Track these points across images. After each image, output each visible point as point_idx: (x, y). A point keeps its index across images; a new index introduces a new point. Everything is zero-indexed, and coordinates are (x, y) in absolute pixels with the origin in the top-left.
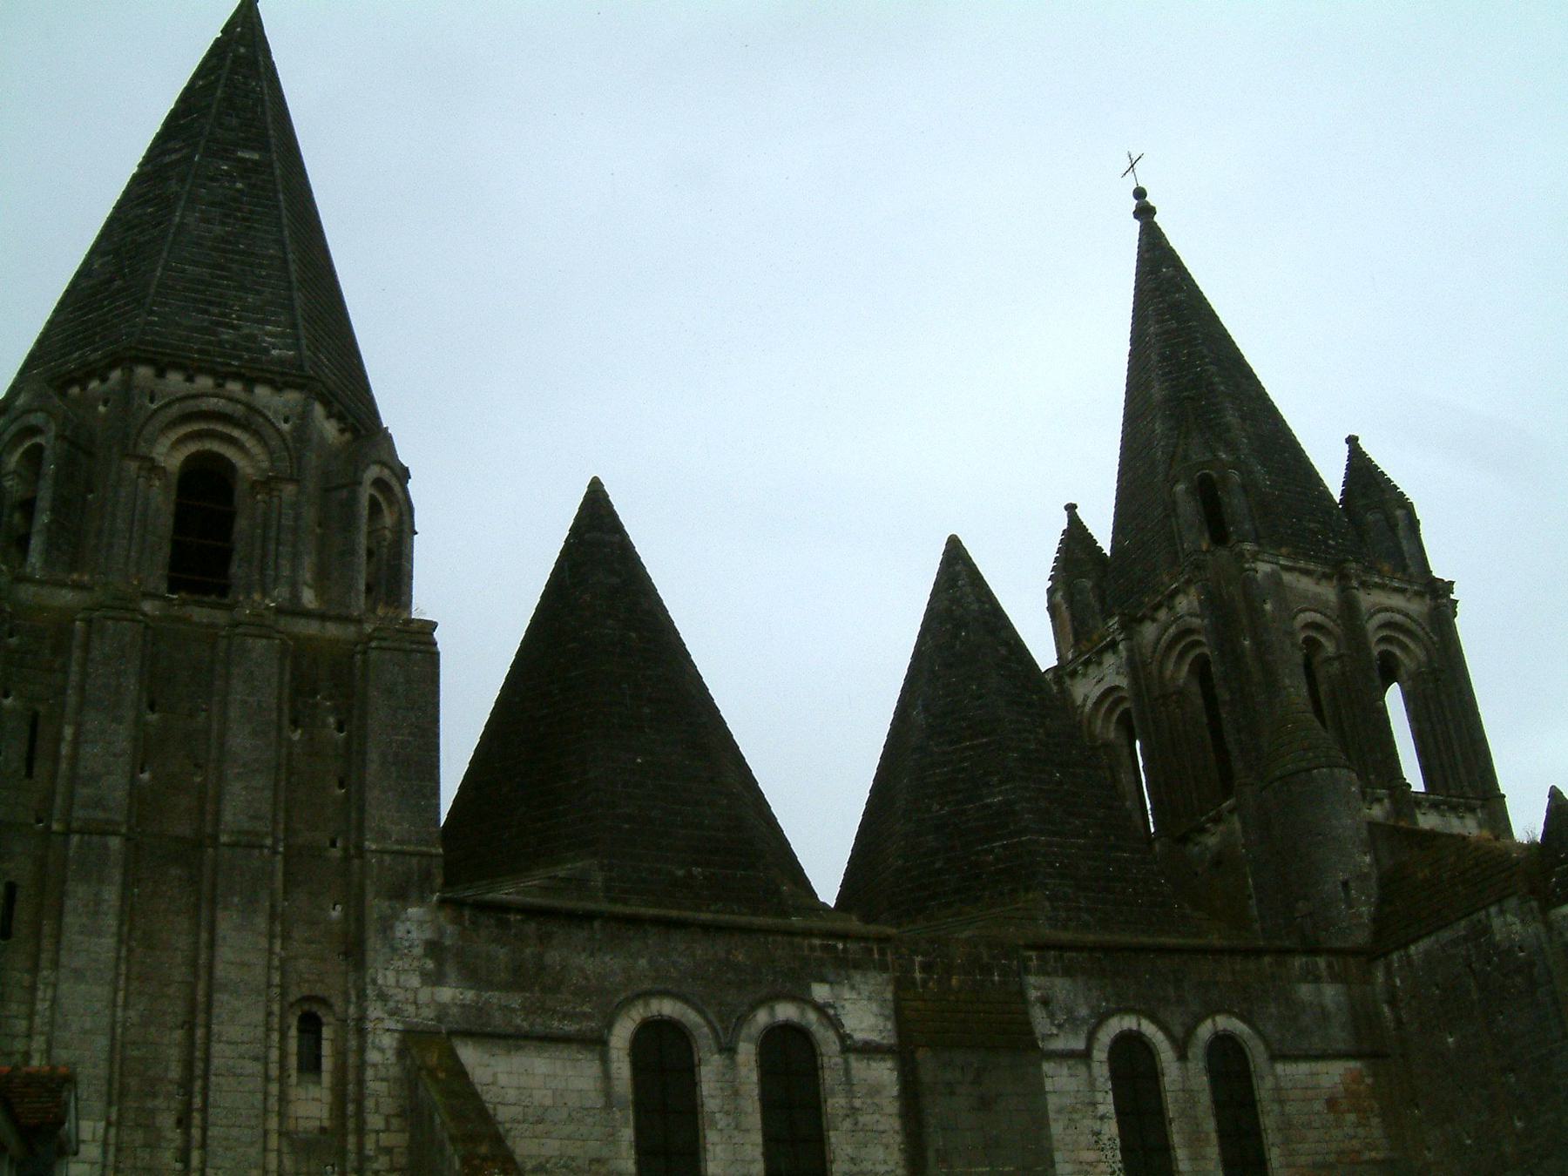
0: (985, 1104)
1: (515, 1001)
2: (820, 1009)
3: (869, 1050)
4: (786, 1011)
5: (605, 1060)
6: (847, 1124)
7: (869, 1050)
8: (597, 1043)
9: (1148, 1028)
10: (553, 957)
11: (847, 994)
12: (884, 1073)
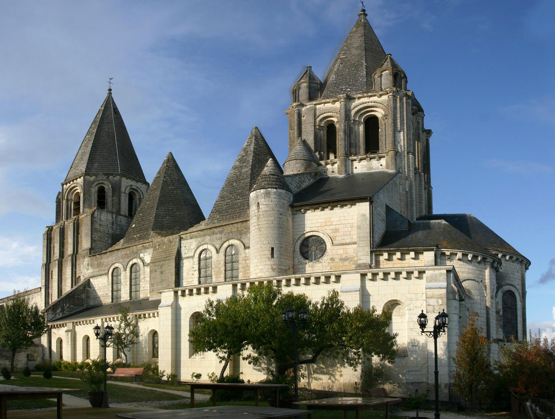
0: (162, 273)
1: (97, 270)
2: (140, 259)
4: (135, 261)
5: (108, 277)
10: (102, 261)
11: (146, 254)
12: (147, 269)
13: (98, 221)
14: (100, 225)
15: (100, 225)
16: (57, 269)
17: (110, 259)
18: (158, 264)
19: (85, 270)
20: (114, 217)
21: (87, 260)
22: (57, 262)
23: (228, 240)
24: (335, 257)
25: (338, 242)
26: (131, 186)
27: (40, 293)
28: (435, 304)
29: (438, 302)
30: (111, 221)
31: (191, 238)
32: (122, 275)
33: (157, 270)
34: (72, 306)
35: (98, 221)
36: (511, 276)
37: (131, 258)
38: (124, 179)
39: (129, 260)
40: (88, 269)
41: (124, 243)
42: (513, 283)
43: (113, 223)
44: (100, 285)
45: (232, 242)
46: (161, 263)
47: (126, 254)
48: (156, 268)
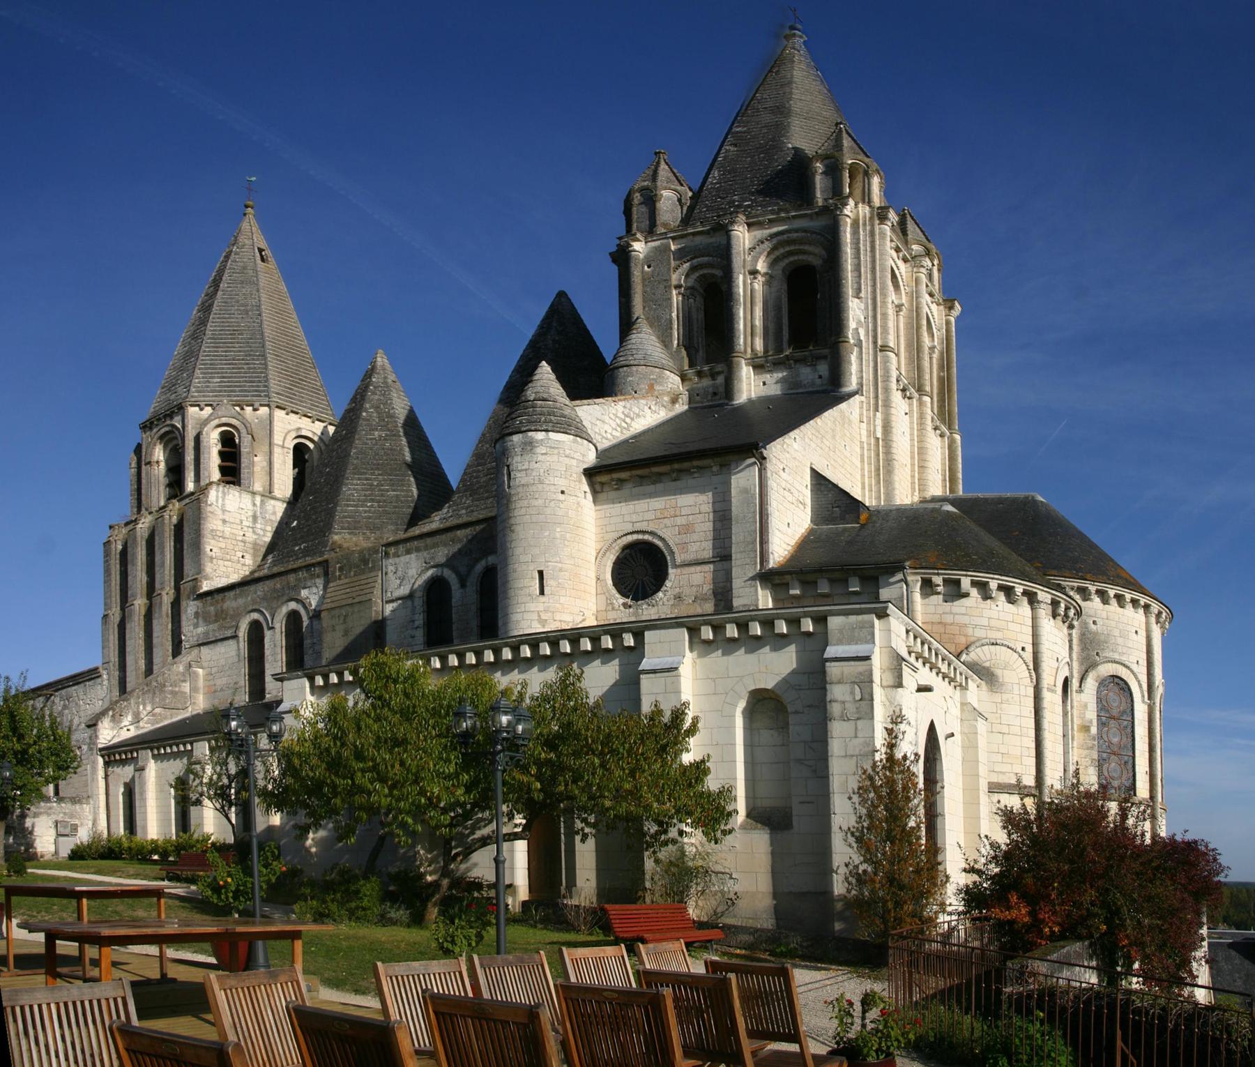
4: (293, 605)
8: (235, 637)
10: (225, 606)
13: (219, 512)
14: (224, 521)
15: (224, 521)
17: (241, 601)
18: (336, 612)
20: (258, 503)
24: (687, 591)
25: (690, 557)
26: (299, 429)
28: (848, 698)
29: (853, 693)
30: (250, 513)
31: (408, 552)
32: (267, 640)
33: (337, 628)
34: (158, 710)
35: (219, 512)
36: (1120, 641)
38: (279, 414)
40: (196, 626)
41: (274, 564)
42: (1124, 659)
43: (255, 518)
44: (222, 662)
47: (275, 590)
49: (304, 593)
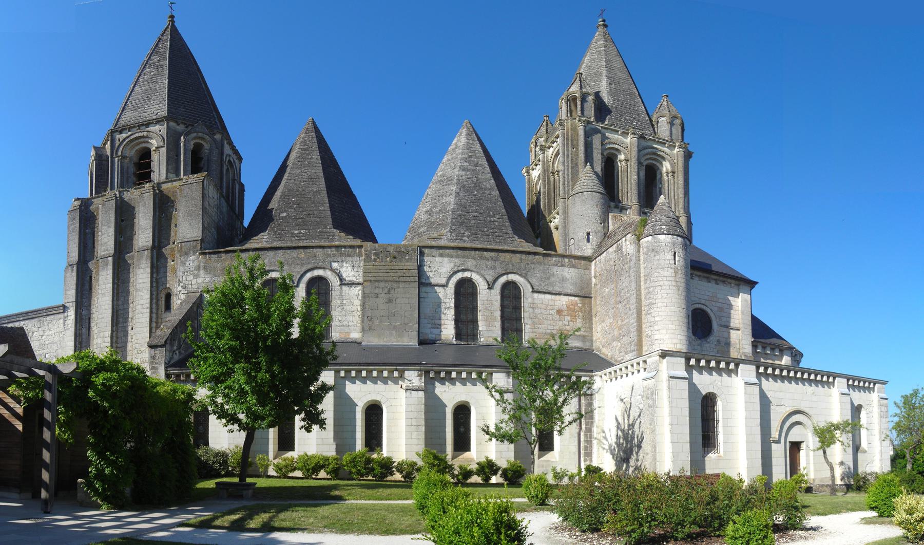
0: (390, 301)
3: (351, 284)
6: (339, 309)
7: (351, 284)
9: (476, 277)
16: (110, 272)
19: (191, 278)
21: (193, 260)
22: (110, 259)
23: (507, 274)
27: (61, 316)
37: (310, 266)
39: (304, 269)
40: (196, 277)
45: (511, 277)
46: (389, 285)
48: (377, 291)
49: (335, 265)
